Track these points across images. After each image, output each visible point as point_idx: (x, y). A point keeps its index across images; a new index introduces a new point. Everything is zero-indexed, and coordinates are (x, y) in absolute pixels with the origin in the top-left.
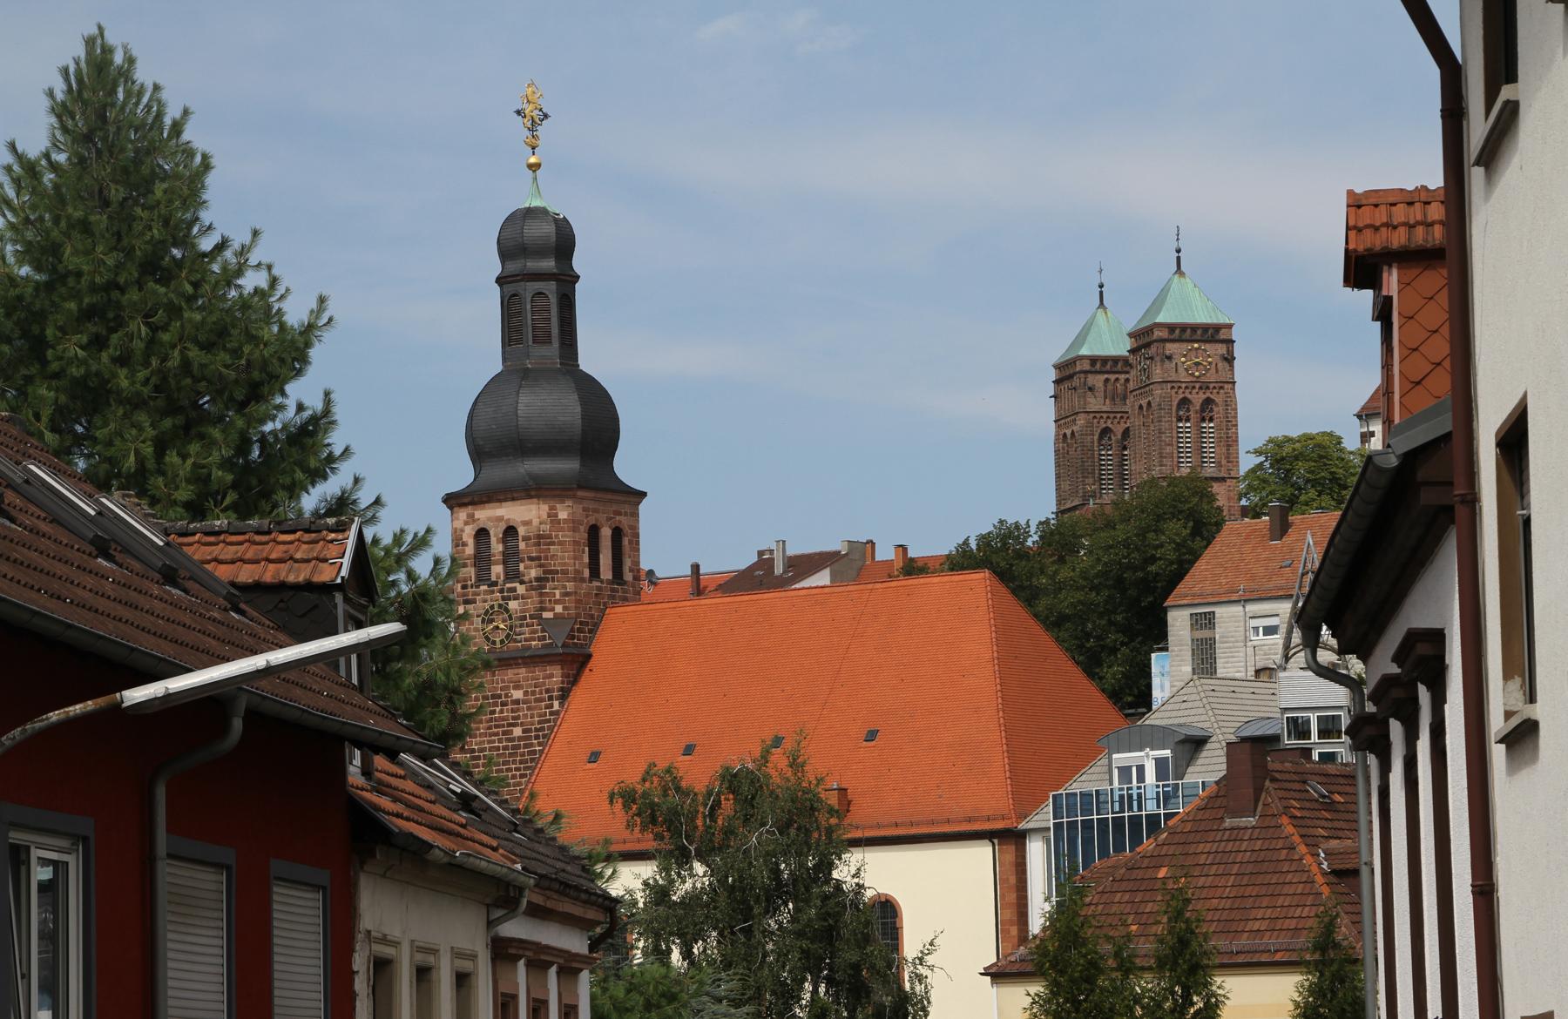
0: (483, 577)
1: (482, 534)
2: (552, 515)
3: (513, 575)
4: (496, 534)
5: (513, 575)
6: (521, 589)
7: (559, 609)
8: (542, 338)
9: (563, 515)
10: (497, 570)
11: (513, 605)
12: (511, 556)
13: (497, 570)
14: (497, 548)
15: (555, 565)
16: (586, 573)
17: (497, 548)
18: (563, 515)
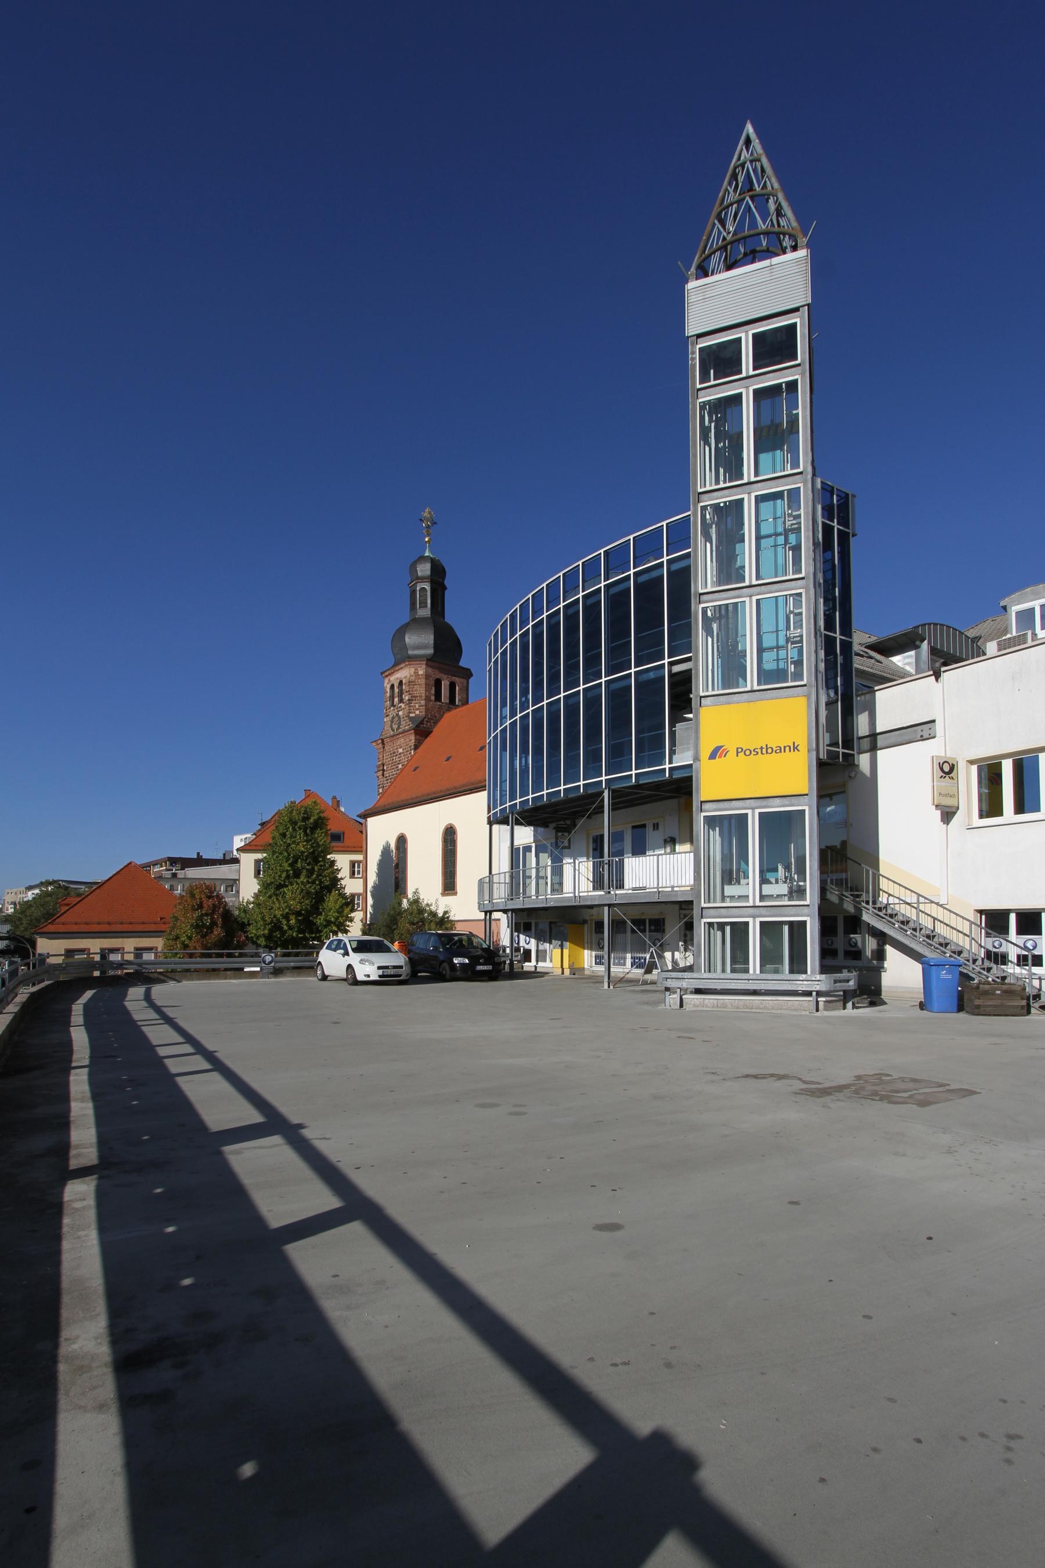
0: (393, 705)
1: (392, 686)
2: (416, 673)
3: (401, 701)
4: (396, 685)
5: (401, 701)
7: (417, 712)
8: (423, 605)
9: (421, 672)
10: (396, 700)
11: (401, 713)
13: (396, 700)
14: (396, 690)
15: (416, 694)
16: (433, 698)
17: (396, 690)
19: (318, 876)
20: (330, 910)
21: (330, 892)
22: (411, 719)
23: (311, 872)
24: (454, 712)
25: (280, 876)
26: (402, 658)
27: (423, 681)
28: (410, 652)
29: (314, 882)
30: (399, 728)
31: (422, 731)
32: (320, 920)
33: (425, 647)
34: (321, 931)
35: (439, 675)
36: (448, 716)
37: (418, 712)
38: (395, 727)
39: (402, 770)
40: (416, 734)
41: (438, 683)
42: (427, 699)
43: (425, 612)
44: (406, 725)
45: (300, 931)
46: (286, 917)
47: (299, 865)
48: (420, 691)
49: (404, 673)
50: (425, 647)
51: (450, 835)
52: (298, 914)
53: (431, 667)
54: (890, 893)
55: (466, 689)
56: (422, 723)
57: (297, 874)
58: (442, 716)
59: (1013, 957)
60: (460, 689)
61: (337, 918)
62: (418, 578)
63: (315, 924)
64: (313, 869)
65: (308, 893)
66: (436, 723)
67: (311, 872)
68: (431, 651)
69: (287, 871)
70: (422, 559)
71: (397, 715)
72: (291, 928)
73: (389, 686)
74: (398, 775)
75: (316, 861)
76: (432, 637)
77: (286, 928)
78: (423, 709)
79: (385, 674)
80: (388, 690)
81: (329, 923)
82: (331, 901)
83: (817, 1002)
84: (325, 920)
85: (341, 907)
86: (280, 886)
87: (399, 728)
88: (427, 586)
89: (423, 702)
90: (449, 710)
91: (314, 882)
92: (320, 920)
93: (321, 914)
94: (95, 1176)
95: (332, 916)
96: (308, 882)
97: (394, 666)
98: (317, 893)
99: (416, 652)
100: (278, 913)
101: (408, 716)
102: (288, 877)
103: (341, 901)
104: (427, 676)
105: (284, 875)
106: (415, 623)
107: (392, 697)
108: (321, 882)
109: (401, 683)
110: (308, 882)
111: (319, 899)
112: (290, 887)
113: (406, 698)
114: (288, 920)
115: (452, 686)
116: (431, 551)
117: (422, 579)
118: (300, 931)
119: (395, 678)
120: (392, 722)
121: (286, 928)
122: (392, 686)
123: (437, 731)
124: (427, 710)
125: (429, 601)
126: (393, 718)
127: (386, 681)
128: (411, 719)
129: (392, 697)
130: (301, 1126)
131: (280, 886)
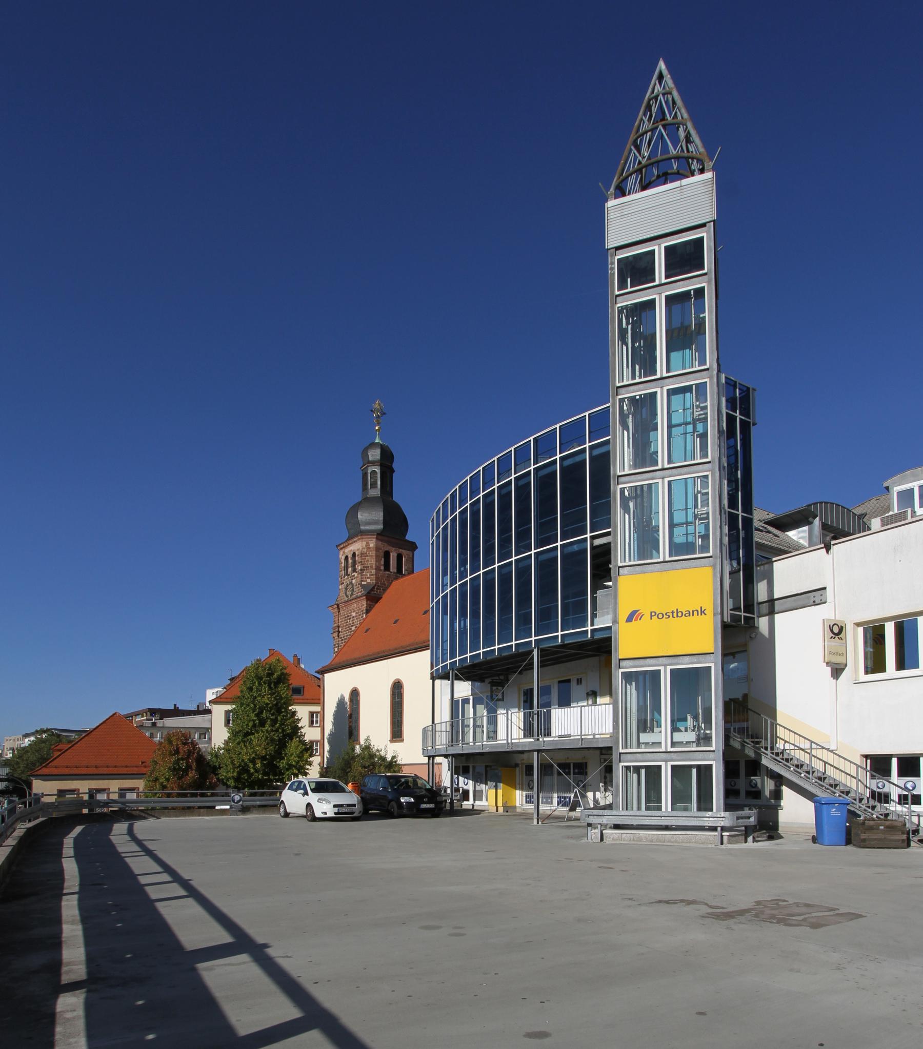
0: (347, 574)
1: (347, 558)
2: (367, 546)
4: (350, 557)
5: (354, 570)
6: (356, 574)
7: (369, 580)
8: (374, 485)
9: (372, 545)
10: (350, 569)
11: (354, 581)
12: (354, 564)
13: (350, 569)
14: (350, 561)
15: (367, 564)
16: (382, 568)
17: (350, 561)
18: (372, 545)
19: (280, 725)
20: (292, 755)
21: (291, 739)
22: (363, 586)
23: (274, 722)
24: (401, 580)
25: (247, 725)
26: (356, 533)
27: (373, 553)
28: (362, 528)
29: (277, 731)
30: (352, 594)
31: (373, 597)
32: (282, 764)
33: (376, 523)
34: (284, 774)
35: (387, 548)
36: (396, 584)
37: (369, 580)
38: (349, 593)
39: (355, 631)
40: (368, 599)
41: (387, 555)
42: (378, 569)
43: (375, 492)
44: (358, 592)
45: (265, 774)
46: (253, 761)
47: (264, 715)
48: (371, 561)
49: (357, 546)
50: (376, 523)
51: (397, 689)
52: (263, 758)
53: (381, 540)
54: (786, 740)
55: (412, 560)
56: (372, 589)
57: (262, 724)
58: (390, 584)
59: (894, 797)
60: (406, 560)
61: (298, 762)
62: (369, 462)
63: (278, 767)
64: (276, 718)
65: (272, 740)
66: (385, 590)
67: (274, 722)
68: (380, 527)
69: (254, 721)
70: (373, 445)
71: (351, 583)
72: (257, 771)
73: (343, 558)
74: (352, 636)
75: (279, 711)
76: (382, 514)
77: (252, 770)
78: (374, 577)
79: (340, 546)
80: (343, 561)
81: (290, 766)
82: (293, 747)
83: (722, 836)
84: (287, 764)
85: (301, 752)
86: (247, 734)
87: (352, 594)
88: (377, 470)
89: (374, 572)
90: (397, 578)
91: (277, 731)
92: (282, 764)
93: (283, 758)
94: (84, 990)
95: (293, 760)
96: (272, 730)
97: (350, 538)
98: (280, 740)
99: (368, 528)
100: (246, 758)
101: (361, 584)
102: (254, 726)
103: (301, 747)
104: (377, 549)
105: (251, 724)
106: (367, 501)
107: (346, 567)
108: (283, 730)
109: (354, 555)
110: (272, 730)
111: (282, 745)
112: (256, 735)
113: (359, 568)
114: (255, 764)
115: (400, 557)
116: (381, 438)
117: (373, 463)
118: (265, 774)
119: (349, 550)
120: (346, 589)
121: (252, 770)
122: (347, 558)
123: (386, 597)
124: (377, 578)
125: (379, 483)
126: (347, 585)
127: (341, 552)
128: (363, 586)
129: (346, 567)
130: (266, 946)
131: (247, 734)
